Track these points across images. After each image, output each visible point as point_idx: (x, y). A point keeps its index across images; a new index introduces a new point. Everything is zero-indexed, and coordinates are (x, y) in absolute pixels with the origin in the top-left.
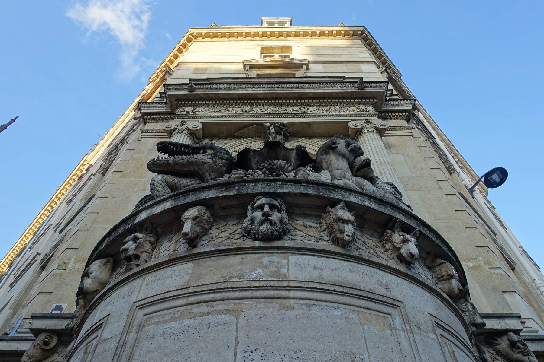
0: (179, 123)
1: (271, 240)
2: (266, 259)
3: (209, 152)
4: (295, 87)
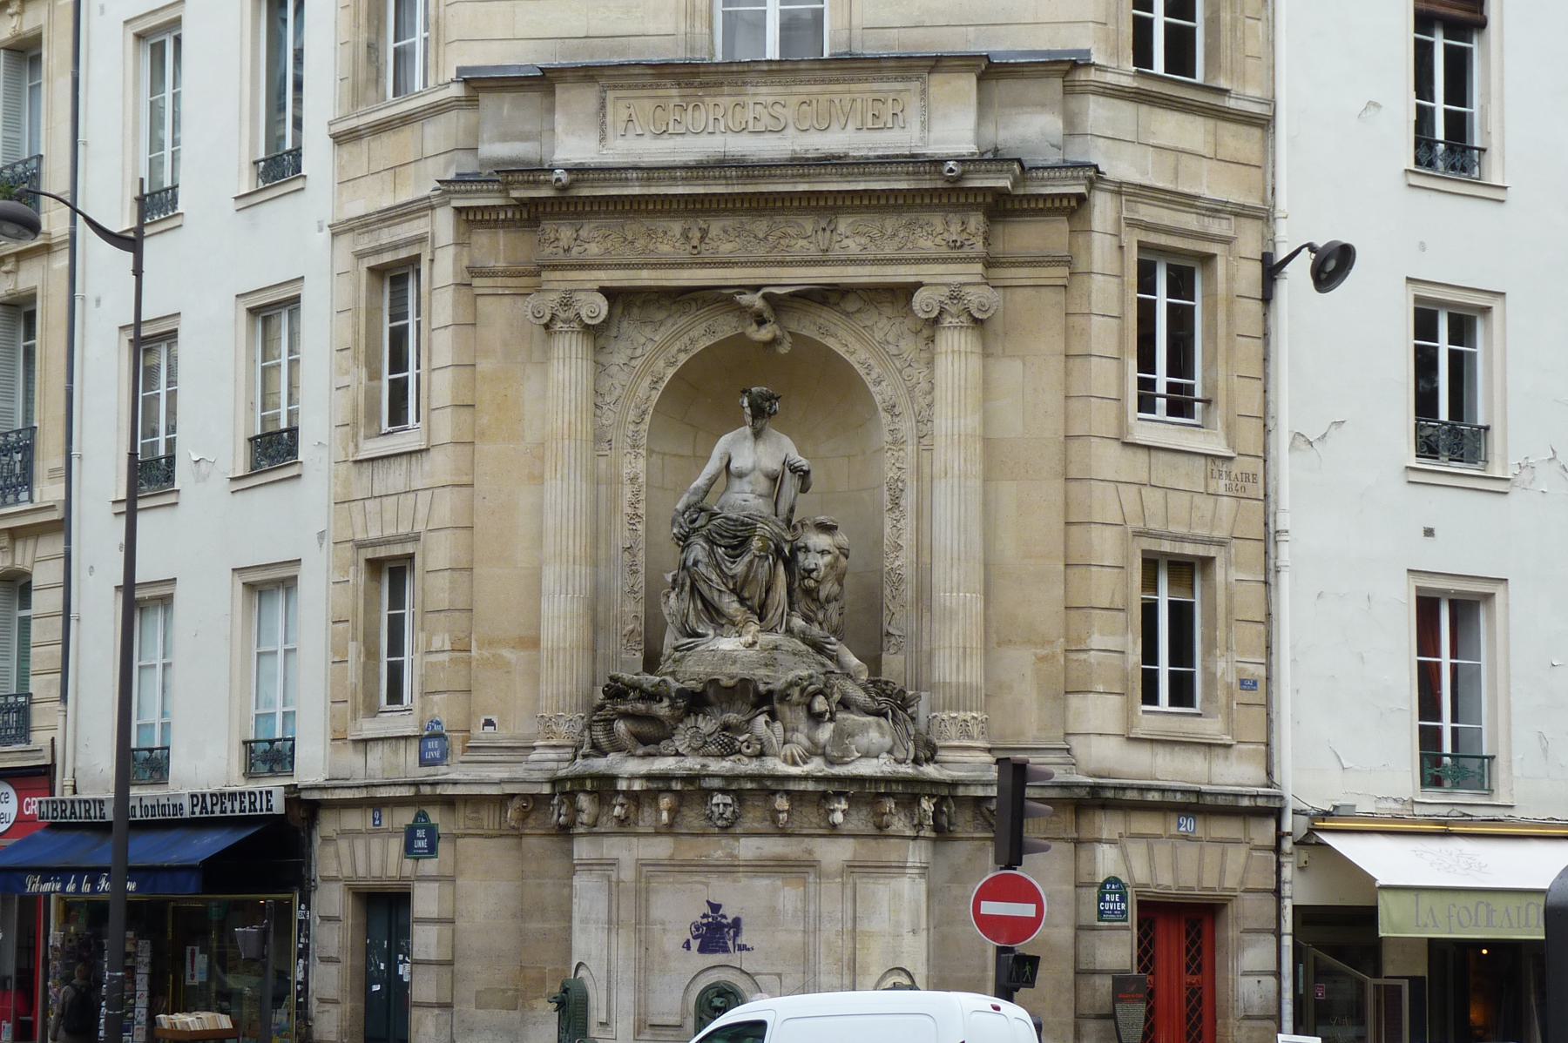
0: (555, 296)
1: (728, 829)
2: (724, 841)
3: (666, 702)
4: (802, 176)
